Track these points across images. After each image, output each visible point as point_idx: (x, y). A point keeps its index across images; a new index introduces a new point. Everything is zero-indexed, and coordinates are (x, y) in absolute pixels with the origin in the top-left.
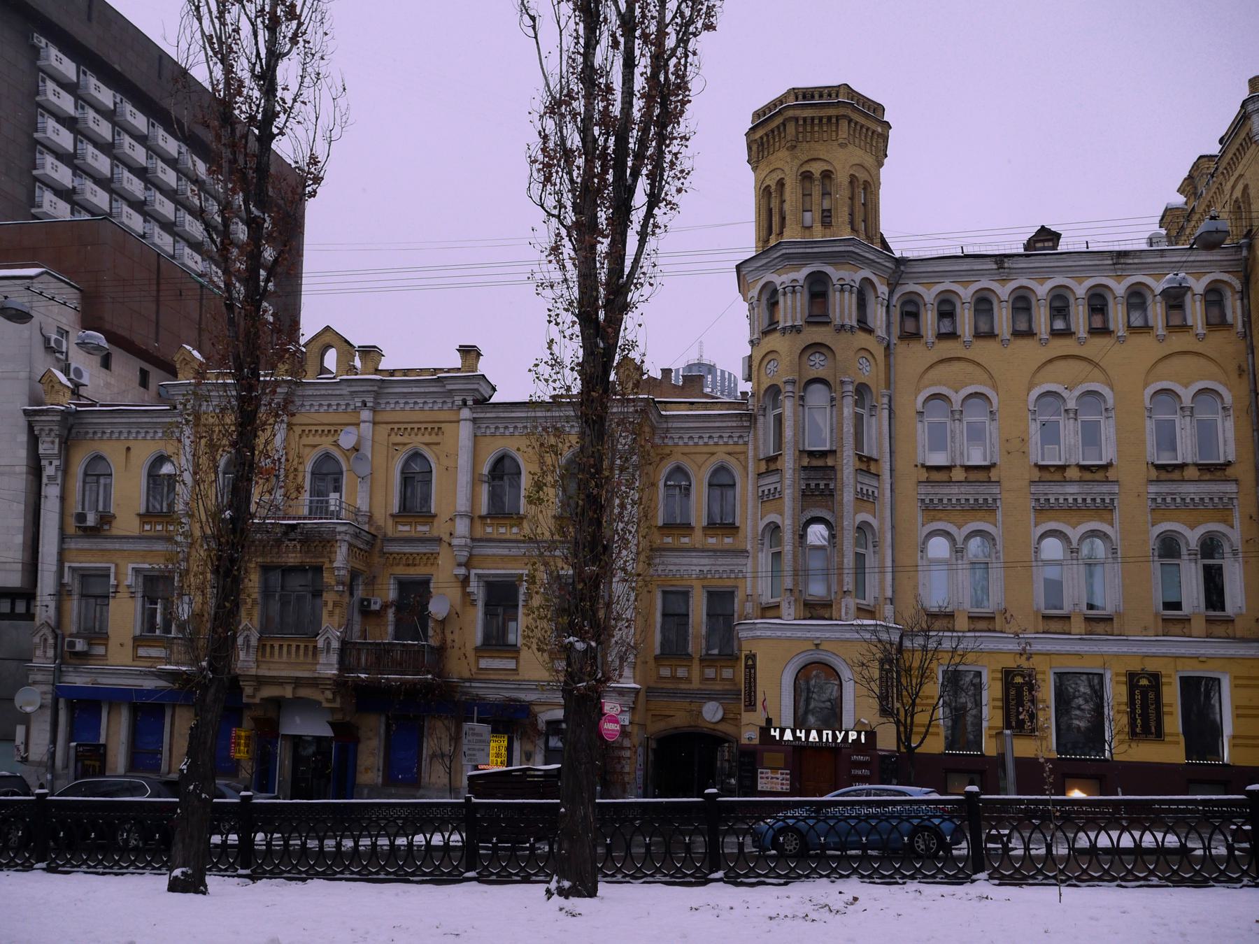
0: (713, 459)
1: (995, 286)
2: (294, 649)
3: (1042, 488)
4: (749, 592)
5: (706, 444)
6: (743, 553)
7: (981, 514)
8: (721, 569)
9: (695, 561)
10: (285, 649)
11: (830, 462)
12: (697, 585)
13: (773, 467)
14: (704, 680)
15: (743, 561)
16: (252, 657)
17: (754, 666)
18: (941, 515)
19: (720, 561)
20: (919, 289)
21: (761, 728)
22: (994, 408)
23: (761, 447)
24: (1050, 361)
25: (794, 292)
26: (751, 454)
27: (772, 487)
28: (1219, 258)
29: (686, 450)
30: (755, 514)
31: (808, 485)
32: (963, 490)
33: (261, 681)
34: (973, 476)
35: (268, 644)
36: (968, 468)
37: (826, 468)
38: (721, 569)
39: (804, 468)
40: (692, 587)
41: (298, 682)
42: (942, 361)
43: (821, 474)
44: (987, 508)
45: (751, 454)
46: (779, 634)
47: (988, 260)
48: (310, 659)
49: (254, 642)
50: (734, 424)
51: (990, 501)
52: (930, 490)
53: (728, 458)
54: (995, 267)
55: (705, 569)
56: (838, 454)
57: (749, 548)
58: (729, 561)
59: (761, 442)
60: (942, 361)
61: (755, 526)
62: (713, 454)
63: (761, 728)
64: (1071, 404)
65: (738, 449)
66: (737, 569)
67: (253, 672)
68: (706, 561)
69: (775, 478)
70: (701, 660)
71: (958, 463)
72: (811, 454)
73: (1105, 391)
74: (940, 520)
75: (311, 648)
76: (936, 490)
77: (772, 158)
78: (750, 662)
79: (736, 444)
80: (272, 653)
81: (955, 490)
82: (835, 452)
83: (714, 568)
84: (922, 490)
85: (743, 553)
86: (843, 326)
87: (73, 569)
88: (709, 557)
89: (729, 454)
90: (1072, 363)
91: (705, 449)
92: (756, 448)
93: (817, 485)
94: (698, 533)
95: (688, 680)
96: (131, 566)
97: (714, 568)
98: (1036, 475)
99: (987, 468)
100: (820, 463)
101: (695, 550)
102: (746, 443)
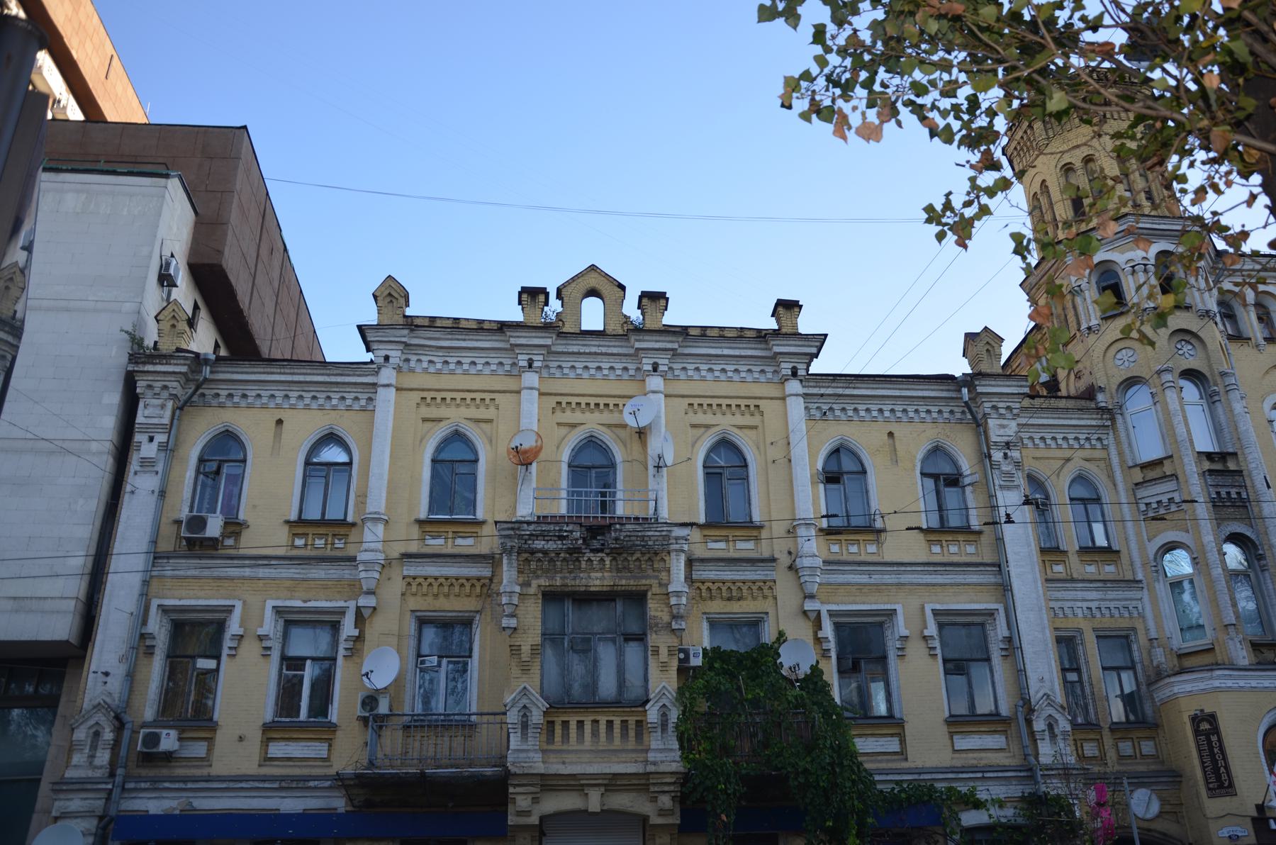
0: (1070, 465)
2: (603, 727)
4: (1153, 634)
5: (1059, 447)
6: (1134, 583)
8: (1112, 605)
9: (1080, 594)
10: (588, 727)
11: (1232, 466)
12: (1087, 627)
13: (1152, 474)
14: (1121, 757)
15: (1138, 594)
16: (533, 742)
17: (1216, 730)
19: (1111, 595)
21: (1254, 819)
23: (1127, 451)
25: (1146, 271)
26: (1115, 460)
27: (1165, 499)
29: (1038, 454)
30: (1138, 534)
31: (1218, 493)
33: (549, 784)
35: (558, 720)
37: (1226, 472)
38: (1112, 605)
39: (1211, 472)
40: (1080, 631)
41: (613, 783)
43: (1229, 480)
45: (1115, 460)
46: (1242, 683)
48: (631, 744)
49: (537, 717)
50: (1094, 423)
53: (1087, 465)
55: (1093, 605)
56: (1241, 458)
57: (1140, 576)
58: (1120, 594)
59: (1125, 446)
61: (1142, 549)
62: (1068, 460)
63: (1254, 819)
65: (1098, 454)
66: (1131, 604)
67: (540, 768)
68: (1094, 595)
69: (1171, 485)
70: (1111, 730)
72: (1209, 456)
75: (632, 725)
77: (1071, 135)
78: (1205, 726)
79: (1093, 448)
80: (566, 736)
82: (1235, 454)
83: (1103, 605)
85: (1134, 583)
86: (1207, 312)
87: (164, 610)
88: (1097, 589)
89: (1087, 460)
91: (1059, 454)
92: (1121, 454)
93: (1228, 493)
94: (1074, 559)
95: (1102, 759)
96: (270, 603)
97: (1103, 605)
100: (1218, 466)
101: (1073, 580)
102: (1105, 448)
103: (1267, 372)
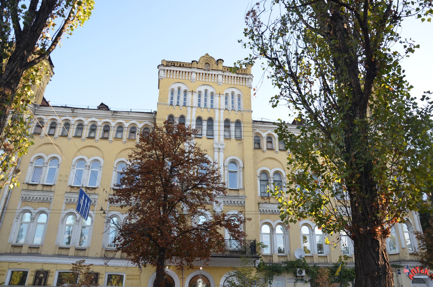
1: (70, 118)
3: (69, 195)
7: (45, 204)
18: (29, 204)
20: (43, 117)
22: (60, 163)
24: (85, 147)
28: (147, 117)
32: (39, 194)
34: (45, 188)
36: (44, 185)
42: (45, 144)
44: (48, 202)
47: (69, 109)
51: (49, 199)
52: (26, 193)
54: (71, 112)
60: (45, 144)
64: (88, 164)
71: (41, 183)
73: (101, 160)
74: (28, 206)
76: (29, 193)
81: (36, 193)
84: (23, 193)
90: (92, 148)
98: (69, 189)
99: (51, 186)
103: (41, 146)
